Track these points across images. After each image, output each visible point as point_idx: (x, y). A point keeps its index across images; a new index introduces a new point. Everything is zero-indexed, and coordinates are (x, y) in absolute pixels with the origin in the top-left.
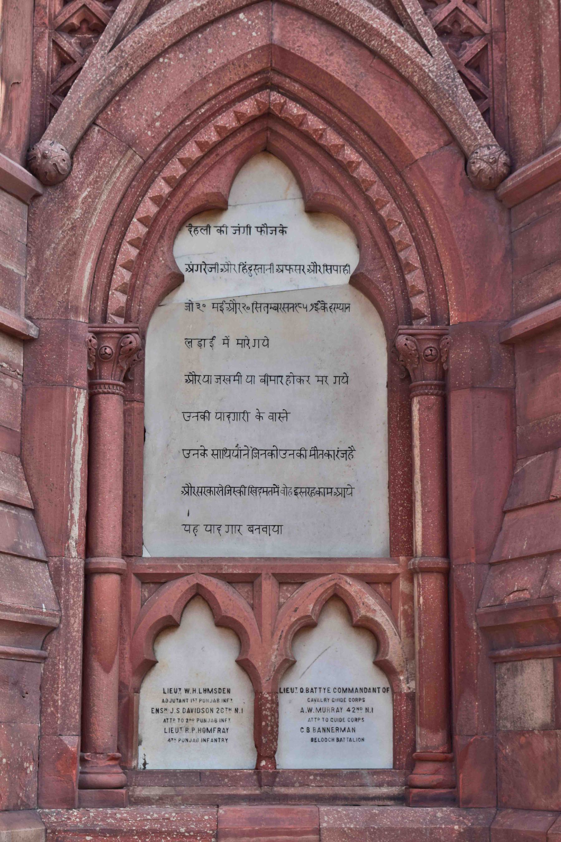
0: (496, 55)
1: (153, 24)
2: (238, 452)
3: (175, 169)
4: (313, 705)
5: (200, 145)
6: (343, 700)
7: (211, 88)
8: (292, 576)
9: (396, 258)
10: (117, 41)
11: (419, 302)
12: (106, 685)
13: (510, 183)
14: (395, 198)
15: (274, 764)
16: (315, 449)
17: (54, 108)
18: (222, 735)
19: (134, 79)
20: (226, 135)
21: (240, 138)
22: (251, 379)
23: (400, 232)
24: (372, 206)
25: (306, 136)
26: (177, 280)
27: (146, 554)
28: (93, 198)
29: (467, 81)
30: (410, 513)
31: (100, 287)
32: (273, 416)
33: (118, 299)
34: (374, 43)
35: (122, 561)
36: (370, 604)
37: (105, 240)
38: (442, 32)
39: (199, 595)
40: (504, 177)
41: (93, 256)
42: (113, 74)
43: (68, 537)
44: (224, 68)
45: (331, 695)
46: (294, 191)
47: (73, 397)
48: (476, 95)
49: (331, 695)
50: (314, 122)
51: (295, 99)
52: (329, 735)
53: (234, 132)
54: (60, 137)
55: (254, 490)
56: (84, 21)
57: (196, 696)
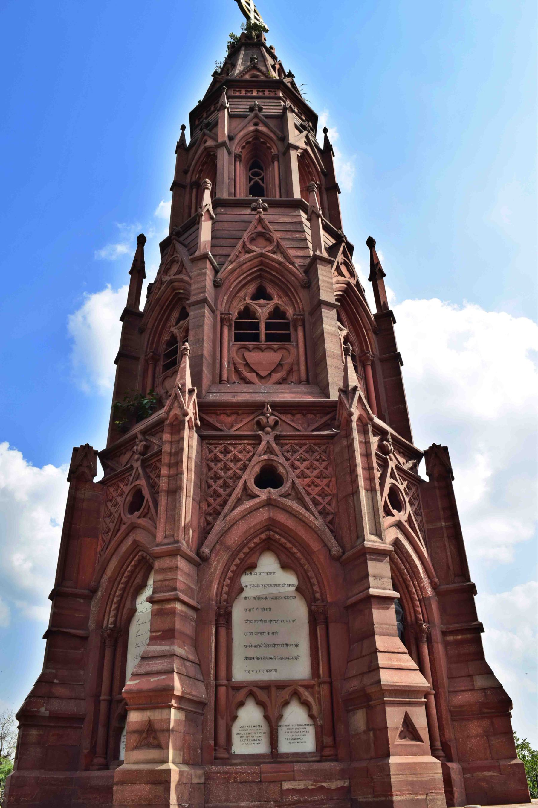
0: (337, 519)
1: (235, 513)
2: (262, 646)
3: (242, 555)
4: (288, 730)
5: (249, 548)
6: (299, 729)
7: (252, 531)
8: (281, 686)
9: (310, 582)
10: (225, 517)
11: (318, 595)
12: (222, 723)
13: (343, 558)
14: (309, 563)
15: (277, 752)
16: (287, 644)
17: (206, 538)
18: (259, 742)
19: (229, 528)
20: (257, 545)
21: (261, 545)
22: (266, 621)
23: (311, 573)
24: (302, 566)
25: (281, 545)
26: (242, 590)
27: (233, 680)
28: (217, 565)
29: (329, 527)
30: (318, 664)
31: (219, 592)
32: (273, 633)
33: (224, 596)
34: (301, 517)
35: (227, 682)
36: (306, 695)
37: (221, 578)
38: (320, 513)
39: (251, 694)
40: (341, 556)
41: (217, 583)
42: (223, 527)
43: (210, 673)
44: (256, 525)
45: (295, 727)
46: (277, 561)
47: (212, 628)
48: (332, 531)
49: (295, 727)
50: (283, 540)
51: (277, 533)
52: (294, 741)
53: (259, 544)
54: (207, 546)
55: (267, 658)
56: (214, 511)
57: (251, 728)
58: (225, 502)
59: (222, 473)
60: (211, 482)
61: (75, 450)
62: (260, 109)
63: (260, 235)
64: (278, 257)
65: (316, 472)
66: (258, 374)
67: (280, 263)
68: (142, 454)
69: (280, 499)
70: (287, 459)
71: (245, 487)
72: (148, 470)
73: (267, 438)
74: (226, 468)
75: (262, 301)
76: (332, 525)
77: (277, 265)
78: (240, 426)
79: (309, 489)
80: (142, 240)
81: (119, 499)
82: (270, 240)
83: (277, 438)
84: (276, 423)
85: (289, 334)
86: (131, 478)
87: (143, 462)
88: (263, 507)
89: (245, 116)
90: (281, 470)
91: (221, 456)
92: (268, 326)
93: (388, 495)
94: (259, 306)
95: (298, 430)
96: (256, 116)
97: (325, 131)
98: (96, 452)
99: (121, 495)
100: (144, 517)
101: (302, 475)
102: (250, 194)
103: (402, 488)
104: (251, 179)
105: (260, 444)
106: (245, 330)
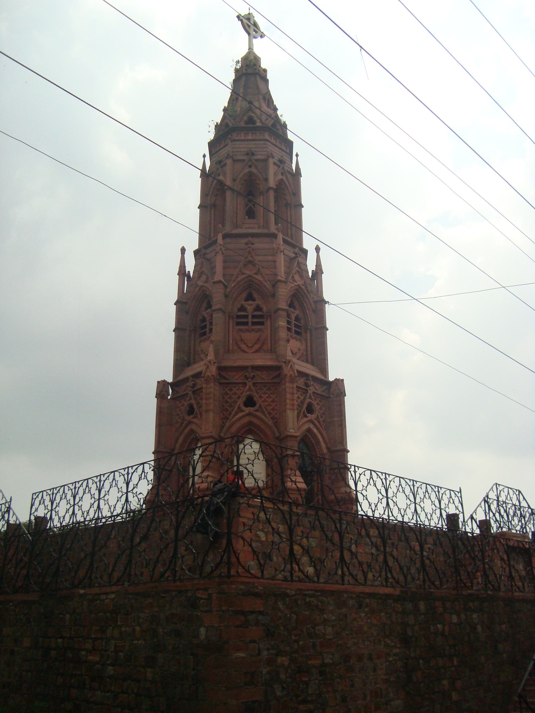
1: (235, 418)
38: (272, 418)
48: (276, 427)
58: (230, 414)
59: (229, 400)
60: (224, 404)
61: (158, 382)
62: (253, 154)
63: (250, 262)
64: (259, 277)
65: (271, 399)
66: (247, 346)
67: (260, 281)
68: (193, 387)
69: (254, 412)
70: (258, 393)
71: (239, 407)
72: (196, 396)
73: (249, 384)
74: (230, 398)
75: (250, 302)
76: (276, 424)
77: (258, 282)
78: (237, 377)
79: (267, 408)
80: (183, 250)
81: (182, 408)
82: (254, 265)
83: (254, 384)
84: (254, 376)
85: (264, 322)
86: (188, 399)
87: (194, 392)
88: (247, 415)
89: (243, 161)
90: (255, 399)
91: (229, 392)
92: (253, 317)
93: (307, 408)
94: (249, 305)
95: (264, 379)
96: (250, 160)
97: (297, 155)
98: (168, 383)
99: (183, 405)
100: (195, 417)
101: (265, 401)
102: (247, 215)
103: (315, 403)
104: (247, 205)
105: (246, 386)
106: (240, 320)
